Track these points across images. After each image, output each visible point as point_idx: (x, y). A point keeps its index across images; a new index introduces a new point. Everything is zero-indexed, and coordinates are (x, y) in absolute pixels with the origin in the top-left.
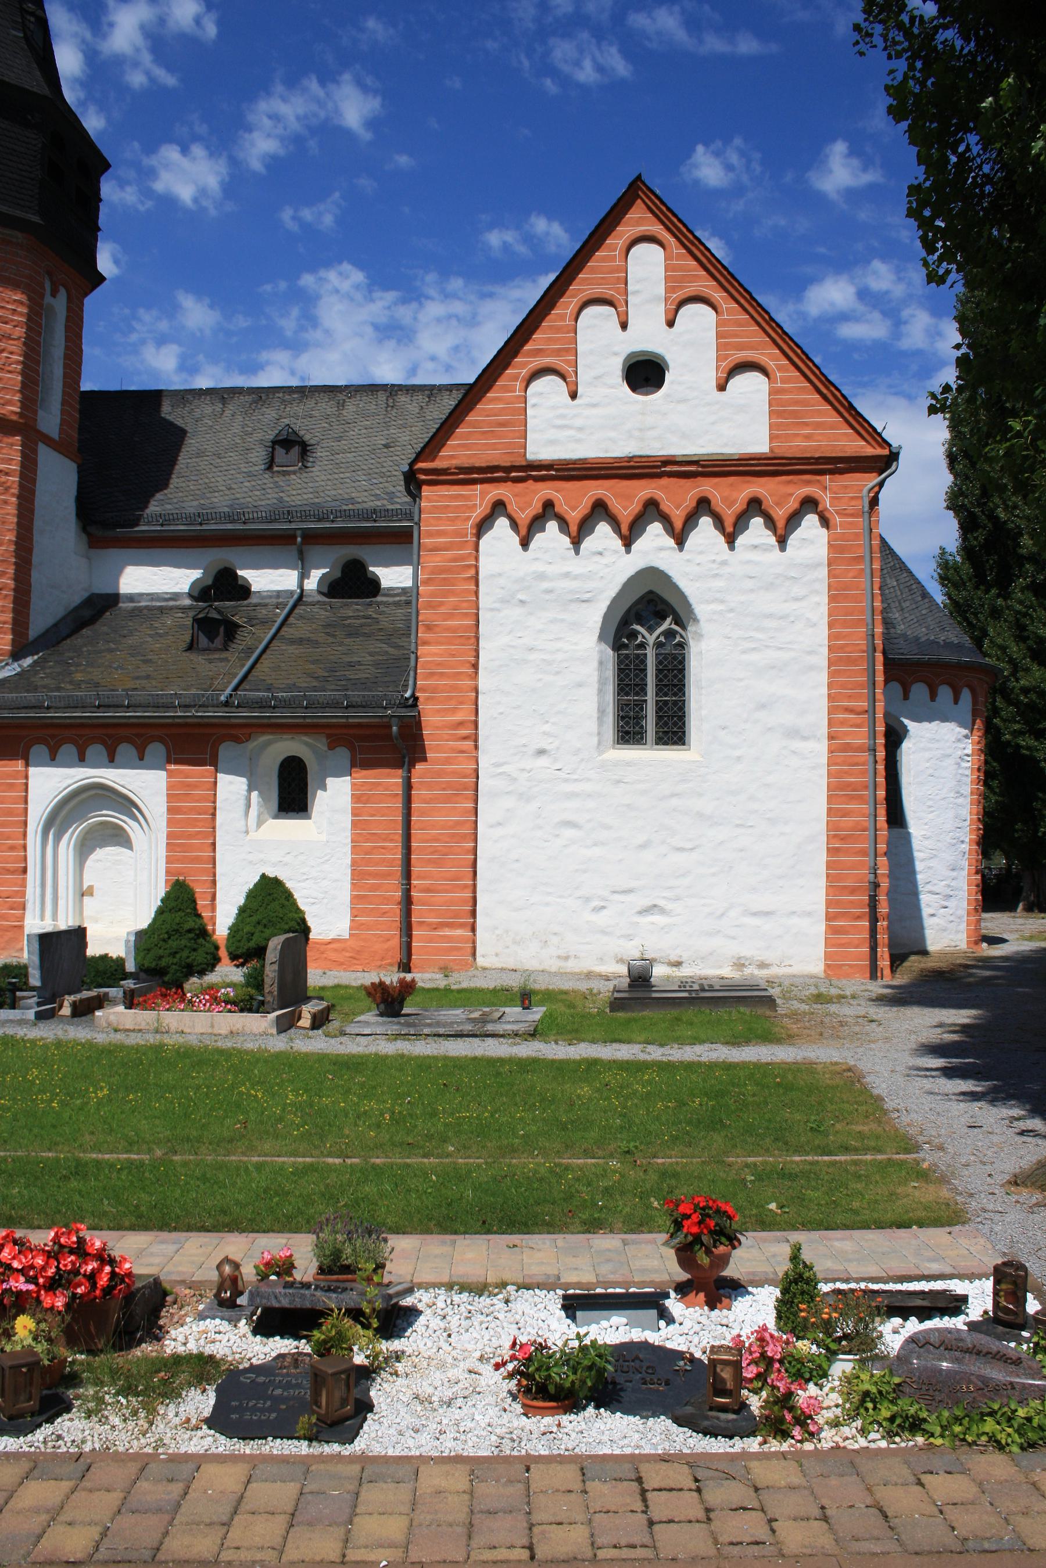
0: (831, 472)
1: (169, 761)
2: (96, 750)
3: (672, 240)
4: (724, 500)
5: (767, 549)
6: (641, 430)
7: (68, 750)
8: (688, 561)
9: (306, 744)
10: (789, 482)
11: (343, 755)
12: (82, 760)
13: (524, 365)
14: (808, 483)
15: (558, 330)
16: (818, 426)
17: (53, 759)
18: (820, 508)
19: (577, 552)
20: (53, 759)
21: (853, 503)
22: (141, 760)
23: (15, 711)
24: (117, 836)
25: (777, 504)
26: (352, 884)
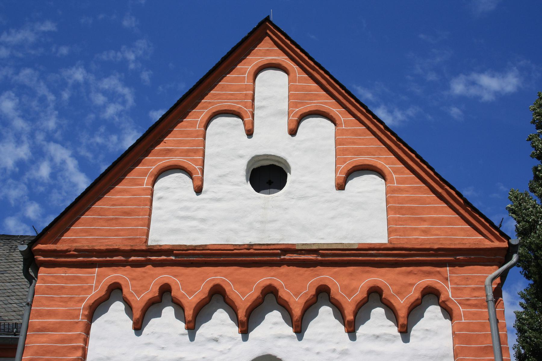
0: (452, 264)
3: (296, 67)
4: (344, 288)
5: (390, 339)
6: (262, 222)
8: (307, 349)
10: (410, 273)
13: (154, 162)
14: (429, 274)
15: (189, 134)
16: (435, 221)
18: (442, 298)
19: (192, 338)
21: (476, 294)
25: (398, 293)
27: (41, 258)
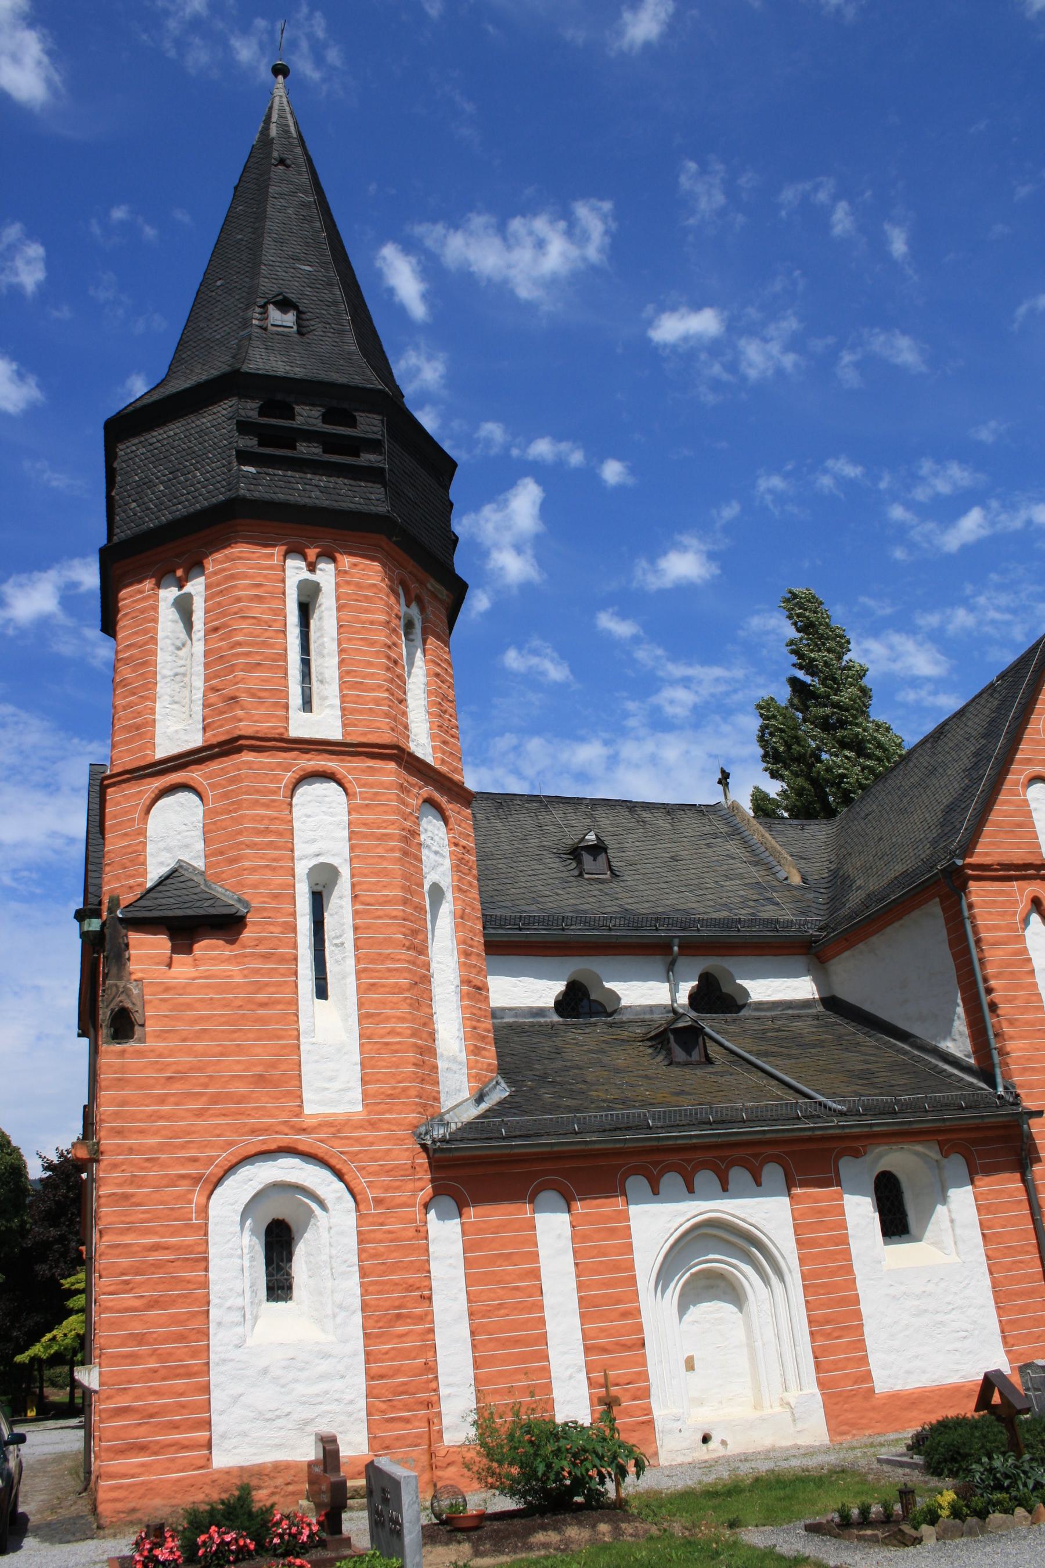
1: (790, 1184)
2: (705, 1178)
7: (672, 1180)
9: (917, 1154)
11: (957, 1164)
17: (655, 1192)
20: (655, 1192)
22: (758, 1184)
23: (618, 1133)
24: (712, 1287)
26: (998, 1308)
27: (970, 872)
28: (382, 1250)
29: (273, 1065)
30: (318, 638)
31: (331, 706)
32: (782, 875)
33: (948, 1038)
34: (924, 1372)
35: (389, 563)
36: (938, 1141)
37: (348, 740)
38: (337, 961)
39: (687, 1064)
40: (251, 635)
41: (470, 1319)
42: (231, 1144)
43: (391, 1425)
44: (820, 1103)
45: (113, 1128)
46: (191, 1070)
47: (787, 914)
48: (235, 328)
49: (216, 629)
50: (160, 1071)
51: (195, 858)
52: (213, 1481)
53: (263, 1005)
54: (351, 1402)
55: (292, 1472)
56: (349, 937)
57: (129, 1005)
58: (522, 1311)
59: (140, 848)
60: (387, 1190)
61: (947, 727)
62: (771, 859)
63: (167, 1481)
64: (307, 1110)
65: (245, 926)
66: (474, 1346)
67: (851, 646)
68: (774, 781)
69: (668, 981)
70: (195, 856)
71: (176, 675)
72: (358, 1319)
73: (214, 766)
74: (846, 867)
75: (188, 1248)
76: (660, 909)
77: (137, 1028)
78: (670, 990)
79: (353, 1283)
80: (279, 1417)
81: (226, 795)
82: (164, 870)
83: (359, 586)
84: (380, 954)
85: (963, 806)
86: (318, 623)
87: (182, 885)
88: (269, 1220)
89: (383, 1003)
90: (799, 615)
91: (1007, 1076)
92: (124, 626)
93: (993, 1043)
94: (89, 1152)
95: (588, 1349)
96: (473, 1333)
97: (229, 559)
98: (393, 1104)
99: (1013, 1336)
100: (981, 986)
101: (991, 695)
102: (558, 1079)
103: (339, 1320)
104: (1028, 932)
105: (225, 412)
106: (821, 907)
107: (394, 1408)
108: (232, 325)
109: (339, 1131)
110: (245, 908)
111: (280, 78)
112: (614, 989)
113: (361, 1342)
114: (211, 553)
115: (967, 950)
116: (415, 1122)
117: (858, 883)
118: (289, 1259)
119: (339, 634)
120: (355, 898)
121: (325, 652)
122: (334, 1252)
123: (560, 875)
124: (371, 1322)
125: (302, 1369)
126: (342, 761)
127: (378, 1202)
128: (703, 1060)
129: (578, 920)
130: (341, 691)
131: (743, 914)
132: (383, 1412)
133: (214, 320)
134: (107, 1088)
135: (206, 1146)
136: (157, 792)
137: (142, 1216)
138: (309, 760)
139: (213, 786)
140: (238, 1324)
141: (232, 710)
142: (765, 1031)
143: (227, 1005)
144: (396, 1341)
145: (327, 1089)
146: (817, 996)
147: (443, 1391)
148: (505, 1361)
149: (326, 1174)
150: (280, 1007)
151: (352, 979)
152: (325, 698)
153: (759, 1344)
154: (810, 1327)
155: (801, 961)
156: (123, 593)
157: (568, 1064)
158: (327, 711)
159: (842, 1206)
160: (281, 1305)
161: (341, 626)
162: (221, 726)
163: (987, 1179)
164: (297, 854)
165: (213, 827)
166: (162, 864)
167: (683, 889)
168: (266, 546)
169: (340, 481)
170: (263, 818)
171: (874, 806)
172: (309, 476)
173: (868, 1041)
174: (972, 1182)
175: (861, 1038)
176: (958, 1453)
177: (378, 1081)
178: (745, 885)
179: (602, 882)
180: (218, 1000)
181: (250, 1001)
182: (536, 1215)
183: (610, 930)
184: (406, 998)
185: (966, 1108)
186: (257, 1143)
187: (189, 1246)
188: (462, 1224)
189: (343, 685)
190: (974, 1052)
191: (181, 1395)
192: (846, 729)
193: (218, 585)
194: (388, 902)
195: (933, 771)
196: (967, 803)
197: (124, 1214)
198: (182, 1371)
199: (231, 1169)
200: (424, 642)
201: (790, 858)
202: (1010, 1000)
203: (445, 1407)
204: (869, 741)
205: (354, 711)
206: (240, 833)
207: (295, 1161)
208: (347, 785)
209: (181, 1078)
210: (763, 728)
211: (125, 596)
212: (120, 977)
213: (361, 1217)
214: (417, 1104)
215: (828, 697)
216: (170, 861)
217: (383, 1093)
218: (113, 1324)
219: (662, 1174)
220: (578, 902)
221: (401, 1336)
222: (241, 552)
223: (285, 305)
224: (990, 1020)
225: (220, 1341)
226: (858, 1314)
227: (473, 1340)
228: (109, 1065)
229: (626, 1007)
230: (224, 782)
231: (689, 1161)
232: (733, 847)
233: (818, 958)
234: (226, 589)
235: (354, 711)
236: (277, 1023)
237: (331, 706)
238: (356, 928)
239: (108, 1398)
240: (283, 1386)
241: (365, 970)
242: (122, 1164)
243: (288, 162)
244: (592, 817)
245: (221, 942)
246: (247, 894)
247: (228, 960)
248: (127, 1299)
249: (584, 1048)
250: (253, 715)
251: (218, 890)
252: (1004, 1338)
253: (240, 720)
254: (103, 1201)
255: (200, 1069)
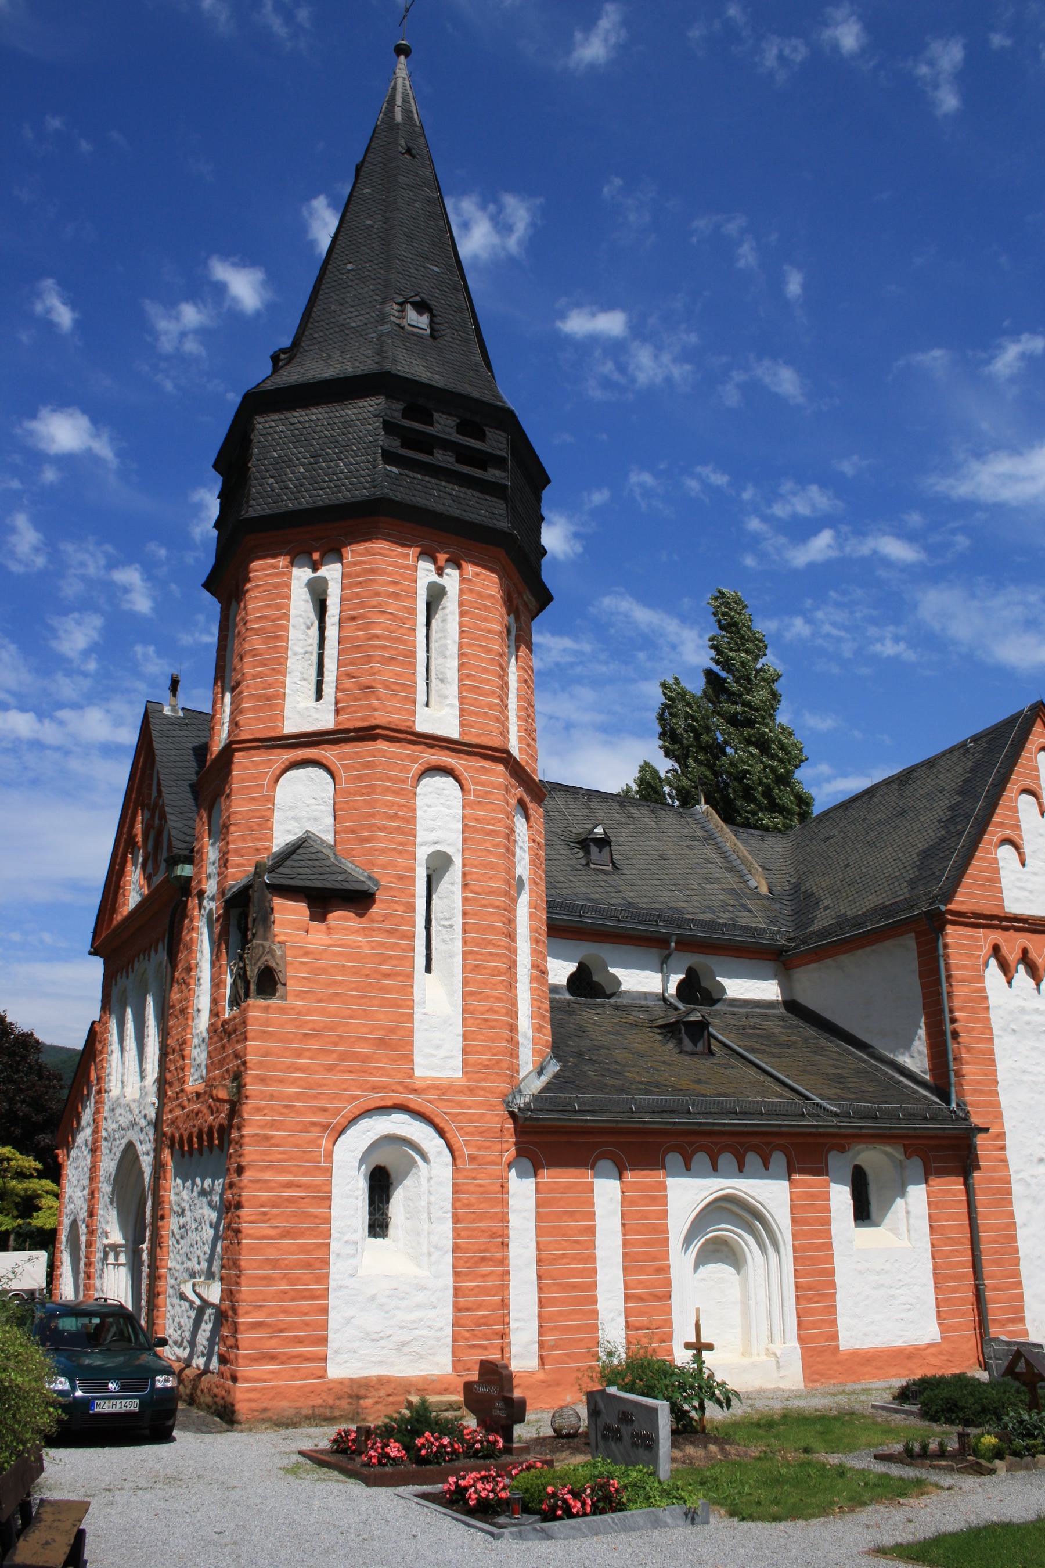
1: (791, 1171)
7: (701, 1159)
11: (916, 1165)
12: (715, 1170)
13: (994, 834)
17: (688, 1169)
20: (688, 1168)
22: (766, 1170)
23: (665, 1115)
26: (936, 1287)
27: (949, 917)
28: (474, 1201)
29: (392, 1030)
30: (440, 638)
31: (451, 705)
32: (753, 883)
33: (907, 1054)
34: (877, 1335)
35: (504, 576)
36: (904, 1145)
37: (467, 739)
38: (444, 941)
39: (693, 1054)
40: (387, 629)
41: (538, 1265)
42: (355, 1098)
43: (472, 1351)
44: (817, 1104)
45: (258, 1075)
46: (325, 1028)
47: (759, 922)
48: (372, 320)
49: (353, 618)
50: (298, 1027)
51: (324, 831)
52: (330, 1389)
53: (386, 976)
54: (441, 1329)
55: (393, 1385)
56: (458, 921)
57: (273, 965)
58: (579, 1262)
59: (268, 813)
60: (479, 1149)
61: (915, 774)
62: (742, 867)
63: (291, 1386)
64: (417, 1073)
65: (373, 902)
66: (540, 1289)
67: (768, 652)
68: (667, 759)
69: (662, 972)
70: (324, 829)
71: (306, 653)
72: (449, 1259)
73: (349, 748)
74: (808, 884)
75: (316, 1187)
76: (657, 906)
77: (279, 986)
78: (663, 981)
79: (446, 1227)
80: (382, 1338)
81: (359, 778)
82: (291, 838)
83: (480, 595)
84: (484, 939)
85: (942, 855)
86: (441, 625)
87: (313, 856)
88: (373, 1166)
89: (484, 983)
90: (724, 614)
91: (960, 1094)
92: (256, 597)
93: (952, 1066)
94: (229, 1095)
95: (627, 1297)
96: (539, 1277)
97: (368, 552)
98: (489, 1074)
99: (946, 1312)
100: (947, 1015)
101: (964, 755)
102: (594, 1058)
103: (433, 1258)
104: (988, 972)
105: (371, 409)
106: (788, 918)
107: (475, 1337)
108: (367, 316)
109: (443, 1094)
110: (376, 885)
111: (402, 57)
112: (617, 974)
113: (451, 1279)
114: (350, 544)
115: (938, 982)
116: (505, 1091)
117: (826, 903)
118: (388, 1202)
119: (460, 638)
120: (465, 886)
121: (448, 653)
122: (433, 1199)
123: (570, 862)
124: (461, 1263)
125: (403, 1299)
126: (460, 758)
127: (472, 1158)
128: (706, 1051)
129: (592, 909)
130: (460, 692)
131: (724, 918)
132: (467, 1339)
133: (347, 305)
134: (254, 1039)
135: (334, 1098)
136: (287, 763)
137: (280, 1156)
138: (433, 755)
139: (346, 768)
140: (353, 1256)
141: (367, 698)
142: (744, 1027)
143: (357, 972)
144: (480, 1279)
145: (434, 1055)
146: (780, 999)
147: (513, 1325)
148: (564, 1302)
149: (430, 1131)
150: (400, 978)
151: (459, 959)
152: (446, 697)
153: (752, 1302)
154: (796, 1291)
155: (770, 966)
156: (255, 565)
157: (596, 1043)
158: (447, 710)
159: (829, 1192)
160: (380, 1240)
161: (463, 631)
162: (356, 712)
163: (938, 1180)
164: (418, 840)
165: (345, 806)
166: (289, 832)
167: (673, 888)
168: (403, 545)
169: (469, 492)
170: (393, 803)
171: (835, 831)
172: (443, 483)
173: (833, 1046)
174: (926, 1182)
175: (823, 1042)
176: (956, 1405)
177: (478, 1052)
178: (723, 889)
179: (606, 873)
180: (349, 967)
181: (376, 971)
182: (596, 1180)
183: (619, 921)
184: (504, 981)
185: (932, 1119)
186: (376, 1098)
187: (317, 1186)
188: (537, 1183)
189: (462, 687)
190: (931, 1070)
191: (306, 1314)
192: (753, 728)
193: (357, 576)
194: (492, 892)
195: (902, 813)
196: (947, 853)
197: (265, 1153)
198: (306, 1294)
199: (354, 1120)
200: (517, 650)
201: (760, 869)
202: (969, 1030)
203: (514, 1338)
204: (773, 742)
205: (472, 713)
206: (372, 815)
207: (405, 1117)
208: (463, 781)
209: (316, 1036)
210: (665, 707)
211: (257, 568)
212: (266, 939)
213: (456, 1170)
214: (507, 1075)
215: (740, 695)
216: (297, 830)
217: (480, 1063)
218: (253, 1250)
219: (694, 1152)
220: (589, 891)
221: (485, 1276)
222: (381, 548)
223: (421, 307)
224: (952, 1046)
225: (337, 1270)
226: (833, 1284)
227: (539, 1283)
228: (256, 1018)
229: (626, 992)
230: (358, 766)
231: (716, 1144)
232: (709, 851)
233: (784, 964)
234: (365, 581)
235: (472, 713)
236: (398, 993)
237: (451, 705)
238: (465, 914)
239: (247, 1313)
240: (387, 1312)
241: (471, 952)
242: (264, 1108)
243: (414, 152)
244: (589, 807)
245: (352, 915)
246: (377, 872)
247: (357, 932)
248: (264, 1228)
249: (603, 1028)
250: (387, 706)
251: (348, 865)
252: (938, 1312)
253: (375, 710)
254: (246, 1140)
255: (332, 1029)
